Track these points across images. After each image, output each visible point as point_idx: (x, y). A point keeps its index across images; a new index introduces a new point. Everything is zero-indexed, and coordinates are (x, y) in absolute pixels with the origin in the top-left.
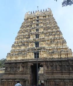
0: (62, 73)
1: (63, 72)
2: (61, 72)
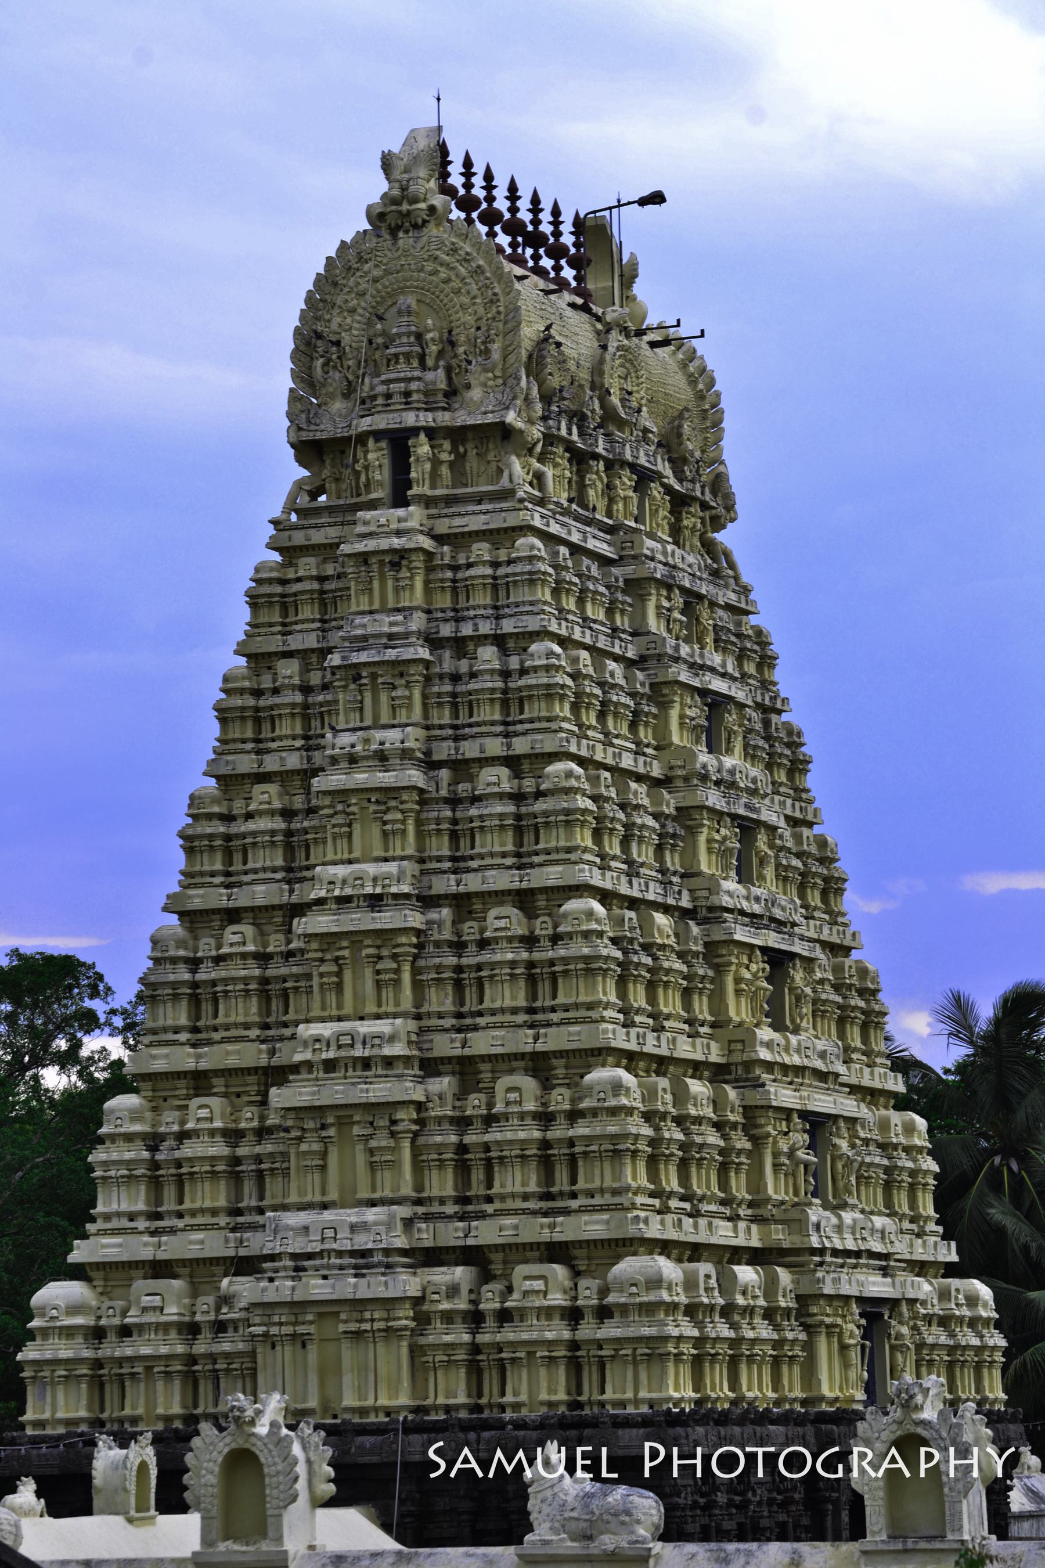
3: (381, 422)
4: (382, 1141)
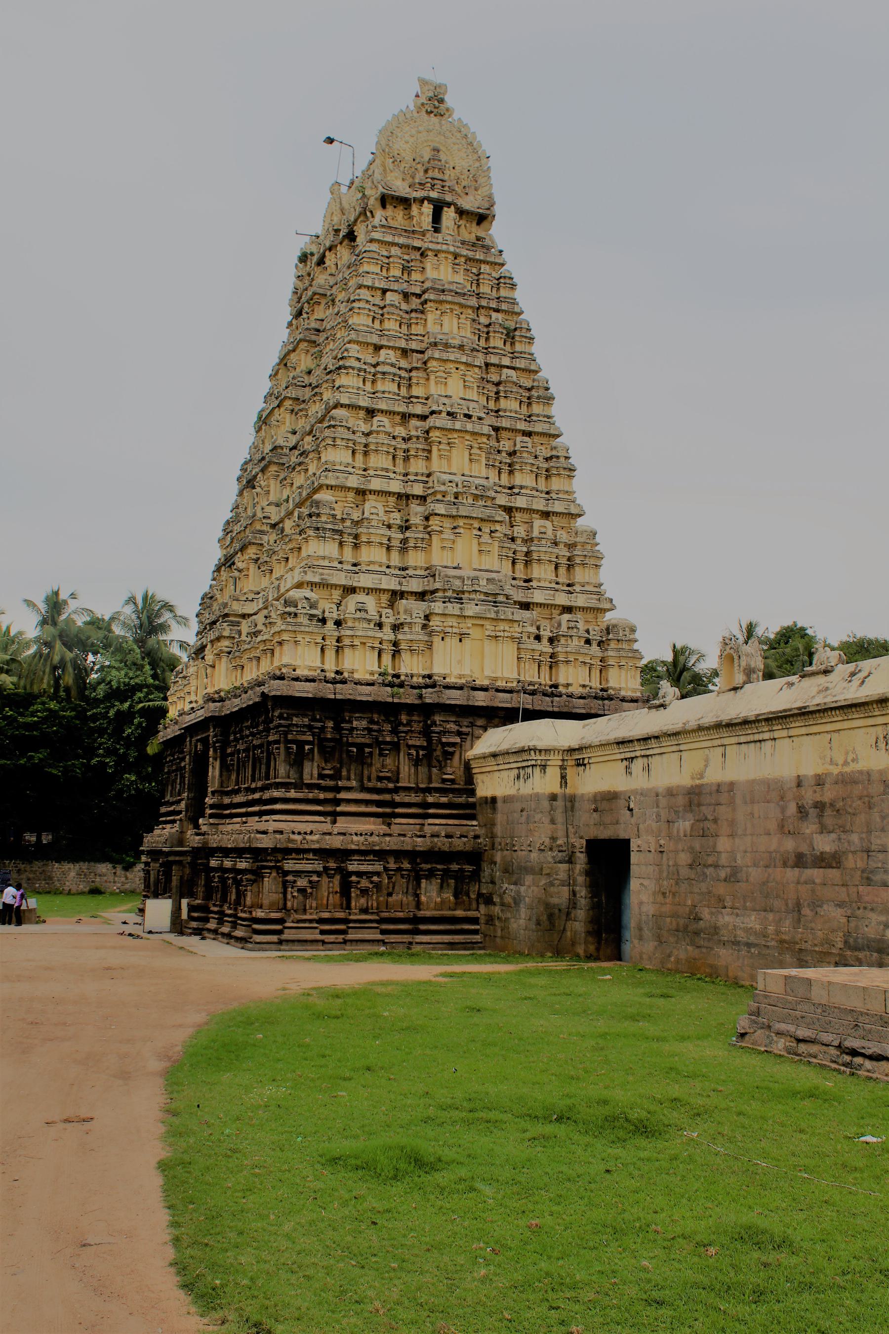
0: (337, 802)
1: (343, 795)
2: (330, 795)
3: (434, 195)
4: (486, 538)
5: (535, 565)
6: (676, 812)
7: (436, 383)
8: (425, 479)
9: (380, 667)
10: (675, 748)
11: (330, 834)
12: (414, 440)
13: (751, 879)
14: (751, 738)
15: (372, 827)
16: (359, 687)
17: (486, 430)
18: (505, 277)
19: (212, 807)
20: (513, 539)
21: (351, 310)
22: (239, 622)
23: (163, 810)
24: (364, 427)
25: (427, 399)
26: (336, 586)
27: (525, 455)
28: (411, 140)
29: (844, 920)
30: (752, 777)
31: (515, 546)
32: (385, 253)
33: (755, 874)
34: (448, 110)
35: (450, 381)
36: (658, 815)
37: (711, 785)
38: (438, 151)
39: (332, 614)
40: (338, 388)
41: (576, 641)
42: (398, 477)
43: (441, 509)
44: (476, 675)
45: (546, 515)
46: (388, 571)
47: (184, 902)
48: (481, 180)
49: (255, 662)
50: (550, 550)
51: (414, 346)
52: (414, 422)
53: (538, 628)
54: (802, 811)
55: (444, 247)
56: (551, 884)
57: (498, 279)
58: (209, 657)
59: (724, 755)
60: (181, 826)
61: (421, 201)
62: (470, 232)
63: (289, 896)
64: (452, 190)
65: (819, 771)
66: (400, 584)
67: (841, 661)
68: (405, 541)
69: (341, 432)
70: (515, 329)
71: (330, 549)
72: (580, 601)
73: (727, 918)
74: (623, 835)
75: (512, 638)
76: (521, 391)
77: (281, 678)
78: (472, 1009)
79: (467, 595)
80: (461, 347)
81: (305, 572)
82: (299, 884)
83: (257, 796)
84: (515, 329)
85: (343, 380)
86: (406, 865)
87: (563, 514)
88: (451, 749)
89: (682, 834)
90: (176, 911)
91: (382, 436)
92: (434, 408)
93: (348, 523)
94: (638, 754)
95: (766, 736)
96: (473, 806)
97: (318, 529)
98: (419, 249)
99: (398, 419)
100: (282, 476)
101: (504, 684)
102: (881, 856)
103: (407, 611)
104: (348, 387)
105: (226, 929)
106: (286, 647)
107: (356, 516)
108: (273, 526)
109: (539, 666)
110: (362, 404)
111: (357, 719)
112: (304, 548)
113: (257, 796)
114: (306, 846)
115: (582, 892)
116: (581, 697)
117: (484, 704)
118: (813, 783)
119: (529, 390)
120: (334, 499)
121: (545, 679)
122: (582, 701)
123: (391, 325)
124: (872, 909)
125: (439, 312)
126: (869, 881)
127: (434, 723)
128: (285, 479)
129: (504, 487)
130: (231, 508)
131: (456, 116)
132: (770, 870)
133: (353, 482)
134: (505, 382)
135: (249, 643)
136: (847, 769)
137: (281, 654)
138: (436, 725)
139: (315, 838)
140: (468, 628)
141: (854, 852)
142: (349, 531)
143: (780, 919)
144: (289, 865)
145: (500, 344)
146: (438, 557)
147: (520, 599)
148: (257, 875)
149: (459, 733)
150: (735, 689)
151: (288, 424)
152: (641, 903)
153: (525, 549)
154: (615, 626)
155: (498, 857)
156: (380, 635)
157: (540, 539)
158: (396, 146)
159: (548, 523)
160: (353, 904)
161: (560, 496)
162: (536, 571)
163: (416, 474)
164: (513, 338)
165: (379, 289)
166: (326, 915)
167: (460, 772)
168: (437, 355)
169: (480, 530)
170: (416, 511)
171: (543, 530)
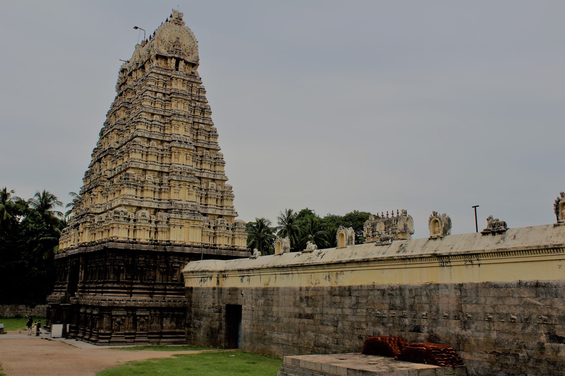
1: (135, 286)
3: (176, 56)
4: (191, 189)
5: (209, 199)
6: (259, 297)
7: (175, 129)
8: (169, 165)
9: (150, 237)
10: (259, 274)
11: (130, 301)
12: (165, 150)
13: (284, 321)
14: (285, 273)
15: (146, 298)
16: (142, 245)
17: (193, 148)
18: (202, 89)
19: (80, 288)
20: (201, 189)
21: (143, 99)
22: (93, 216)
23: (56, 286)
24: (147, 145)
25: (171, 135)
26: (134, 206)
27: (207, 157)
28: (169, 34)
29: (314, 337)
30: (285, 286)
31: (202, 192)
32: (157, 78)
33: (285, 320)
34: (183, 23)
35: (180, 128)
36: (252, 297)
37: (271, 288)
38: (179, 39)
39: (133, 217)
40: (137, 129)
41: (223, 229)
42: (159, 165)
43: (175, 178)
44: (186, 241)
45: (214, 180)
46: (154, 201)
47: (68, 325)
48: (194, 51)
49: (101, 233)
50: (215, 194)
51: (167, 114)
52: (166, 144)
53: (210, 223)
54: (301, 299)
55: (180, 77)
56: (213, 320)
57: (199, 89)
58: (81, 229)
59: (276, 278)
60: (66, 294)
61: (171, 58)
62: (189, 70)
63: (113, 325)
64: (183, 54)
65: (307, 286)
66: (158, 206)
67: (315, 248)
68: (161, 189)
69: (138, 147)
70: (205, 109)
71: (132, 192)
72: (226, 213)
73: (275, 335)
74: (239, 303)
75: (200, 227)
76: (206, 132)
77: (113, 241)
78: (188, 369)
79: (183, 211)
80: (184, 116)
81: (123, 201)
82: (117, 320)
83: (101, 285)
84: (205, 109)
85: (139, 127)
86: (158, 312)
87: (220, 180)
88: (176, 269)
89: (260, 304)
90: (64, 329)
91: (153, 149)
92: (174, 139)
93: (139, 182)
94: (245, 275)
95: (290, 272)
96: (183, 290)
97: (128, 184)
98: (170, 76)
99: (159, 142)
100: (112, 160)
101: (196, 244)
102: (326, 316)
103: (161, 217)
104: (141, 129)
105: (87, 337)
106: (115, 230)
107: (142, 179)
108: (109, 179)
109: (209, 237)
110: (146, 136)
111: (141, 257)
112: (122, 191)
113: (101, 285)
114: (121, 306)
115: (224, 323)
116: (225, 249)
117: (188, 252)
118: (305, 289)
119: (209, 132)
120: (134, 173)
121: (211, 242)
122: (225, 251)
123: (158, 106)
124: (323, 333)
125: (176, 102)
126: (322, 324)
127: (170, 259)
128: (114, 161)
129: (198, 169)
130: (88, 166)
131: (186, 25)
132: (290, 319)
133: (142, 166)
134: (200, 129)
135: (99, 226)
136: (316, 286)
137: (113, 232)
138: (171, 260)
139: (124, 302)
140: (184, 223)
141: (318, 314)
142: (140, 185)
143: (293, 336)
144: (114, 313)
145: (199, 114)
146: (173, 196)
147: (203, 212)
148: (101, 317)
149: (179, 263)
150: (280, 254)
151: (115, 139)
152: (245, 328)
153: (205, 193)
154: (238, 223)
155: (193, 310)
156: (150, 225)
157: (211, 189)
158: (163, 36)
159: (214, 184)
160: (138, 327)
161: (219, 173)
162: (210, 201)
163: (166, 164)
164: (204, 112)
165: (154, 91)
166: (127, 332)
167: (179, 277)
168: (175, 119)
169: (189, 186)
170: (165, 178)
171: (212, 186)
